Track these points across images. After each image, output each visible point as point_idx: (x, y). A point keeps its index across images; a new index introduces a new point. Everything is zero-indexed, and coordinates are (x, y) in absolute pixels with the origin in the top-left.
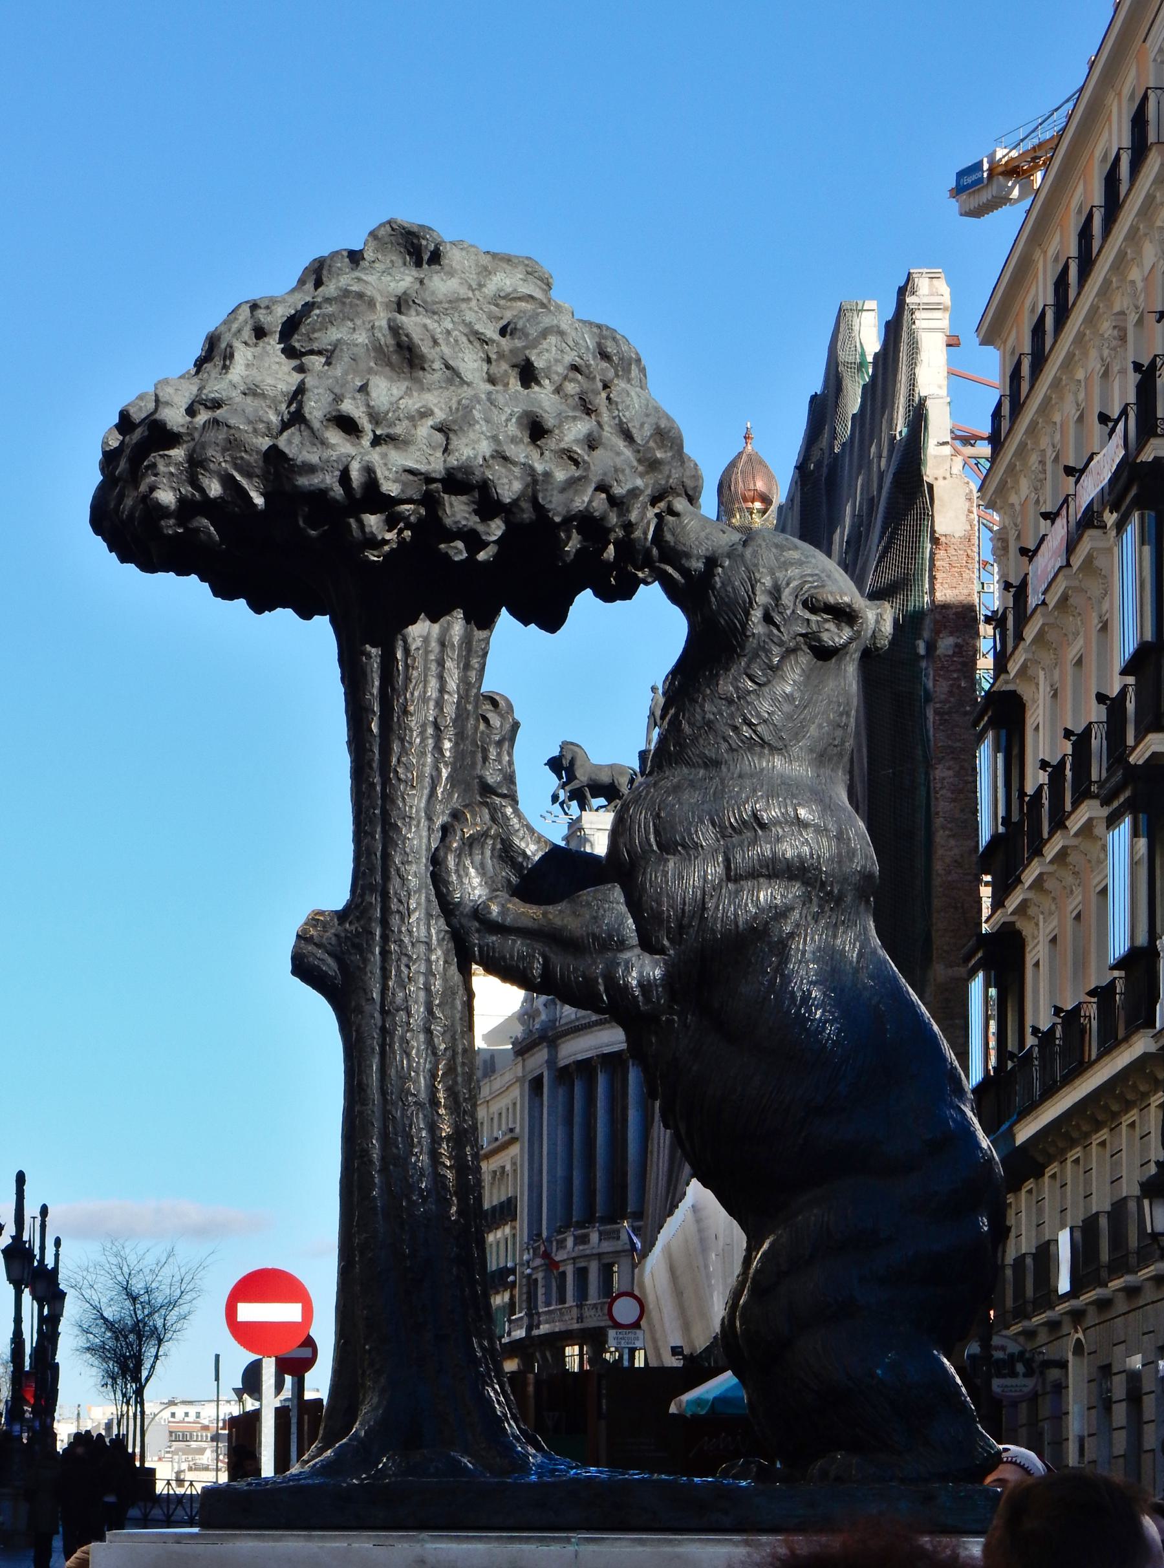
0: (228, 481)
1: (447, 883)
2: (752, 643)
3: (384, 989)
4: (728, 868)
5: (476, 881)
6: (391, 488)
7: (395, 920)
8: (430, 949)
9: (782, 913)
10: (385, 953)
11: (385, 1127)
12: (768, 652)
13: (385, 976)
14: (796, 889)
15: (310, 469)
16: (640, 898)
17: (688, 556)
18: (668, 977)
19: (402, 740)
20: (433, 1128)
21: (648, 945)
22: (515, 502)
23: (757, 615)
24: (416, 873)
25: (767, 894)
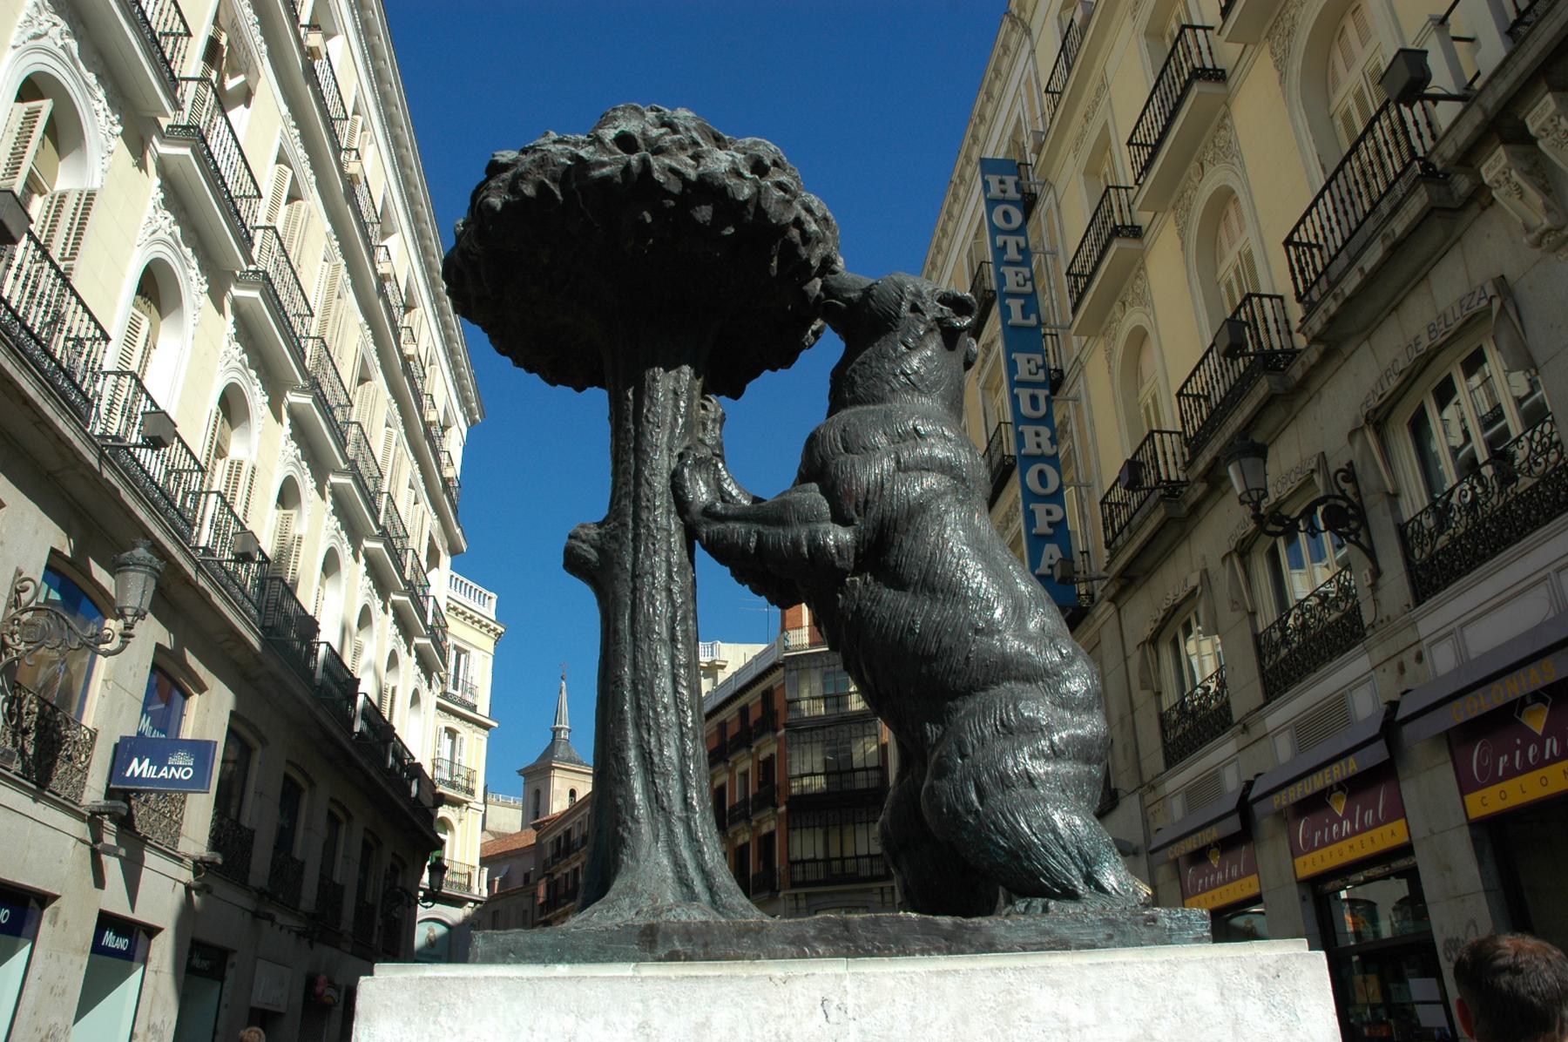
0: (541, 186)
1: (683, 487)
2: (901, 324)
3: (636, 559)
4: (898, 462)
5: (703, 489)
6: (659, 176)
7: (644, 515)
8: (670, 535)
9: (939, 495)
10: (636, 537)
11: (635, 657)
12: (916, 328)
13: (636, 550)
14: (946, 481)
15: (603, 164)
16: (834, 484)
17: (847, 290)
18: (858, 544)
19: (651, 398)
20: (673, 659)
21: (840, 518)
22: (746, 202)
23: (905, 306)
24: (661, 483)
25: (930, 481)
